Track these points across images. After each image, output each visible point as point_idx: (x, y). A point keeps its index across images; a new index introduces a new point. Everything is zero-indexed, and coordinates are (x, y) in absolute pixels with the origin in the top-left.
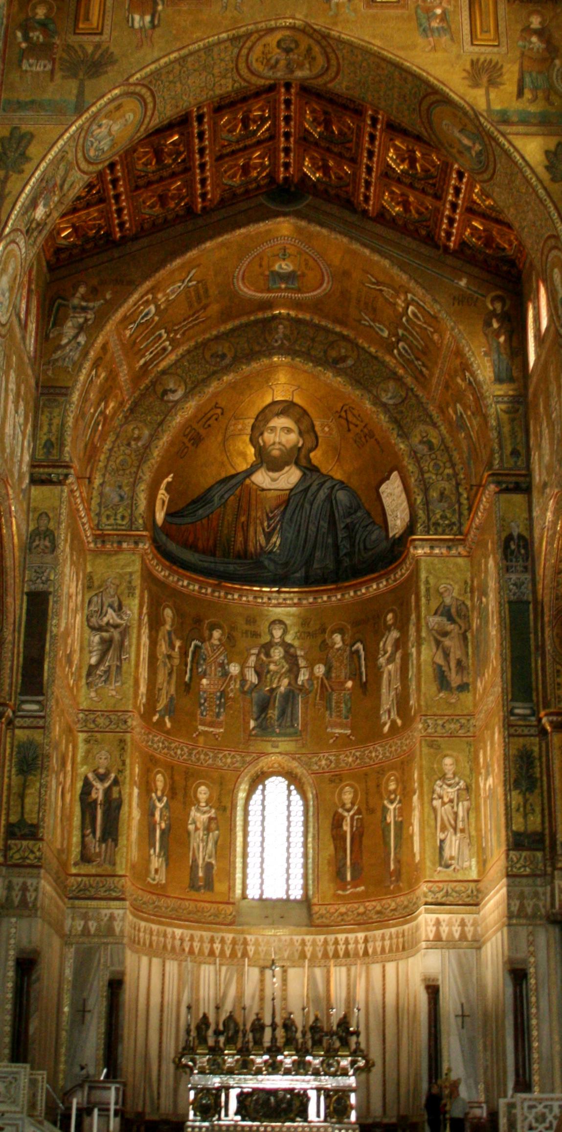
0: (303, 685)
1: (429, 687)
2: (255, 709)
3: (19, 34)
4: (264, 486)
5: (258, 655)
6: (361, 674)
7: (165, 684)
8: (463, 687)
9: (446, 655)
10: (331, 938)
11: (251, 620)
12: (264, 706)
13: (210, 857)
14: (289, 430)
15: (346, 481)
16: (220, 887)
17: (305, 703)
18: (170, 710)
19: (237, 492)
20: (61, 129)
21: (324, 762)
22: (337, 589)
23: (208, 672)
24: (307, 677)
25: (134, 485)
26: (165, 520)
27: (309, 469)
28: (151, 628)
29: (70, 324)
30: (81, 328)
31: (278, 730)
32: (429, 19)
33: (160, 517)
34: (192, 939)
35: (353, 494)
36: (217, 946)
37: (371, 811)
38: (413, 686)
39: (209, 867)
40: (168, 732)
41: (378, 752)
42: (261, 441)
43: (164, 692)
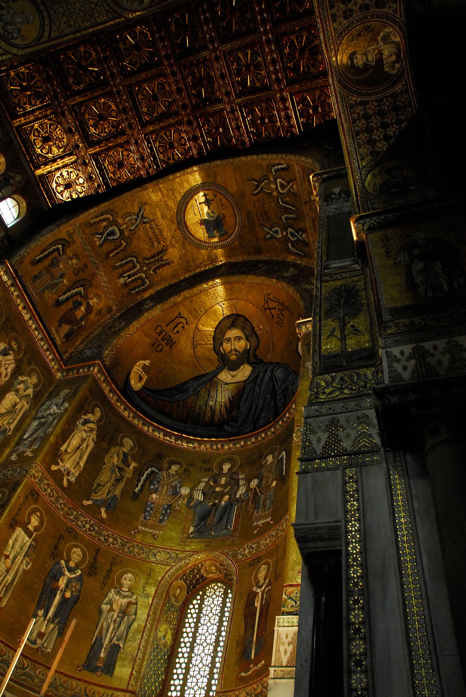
0: (240, 497)
2: (196, 518)
4: (227, 381)
5: (207, 483)
6: (282, 472)
7: (109, 485)
13: (118, 640)
14: (239, 338)
15: (279, 361)
19: (208, 386)
21: (247, 551)
23: (159, 489)
24: (243, 492)
31: (213, 533)
42: (221, 350)
43: (106, 489)
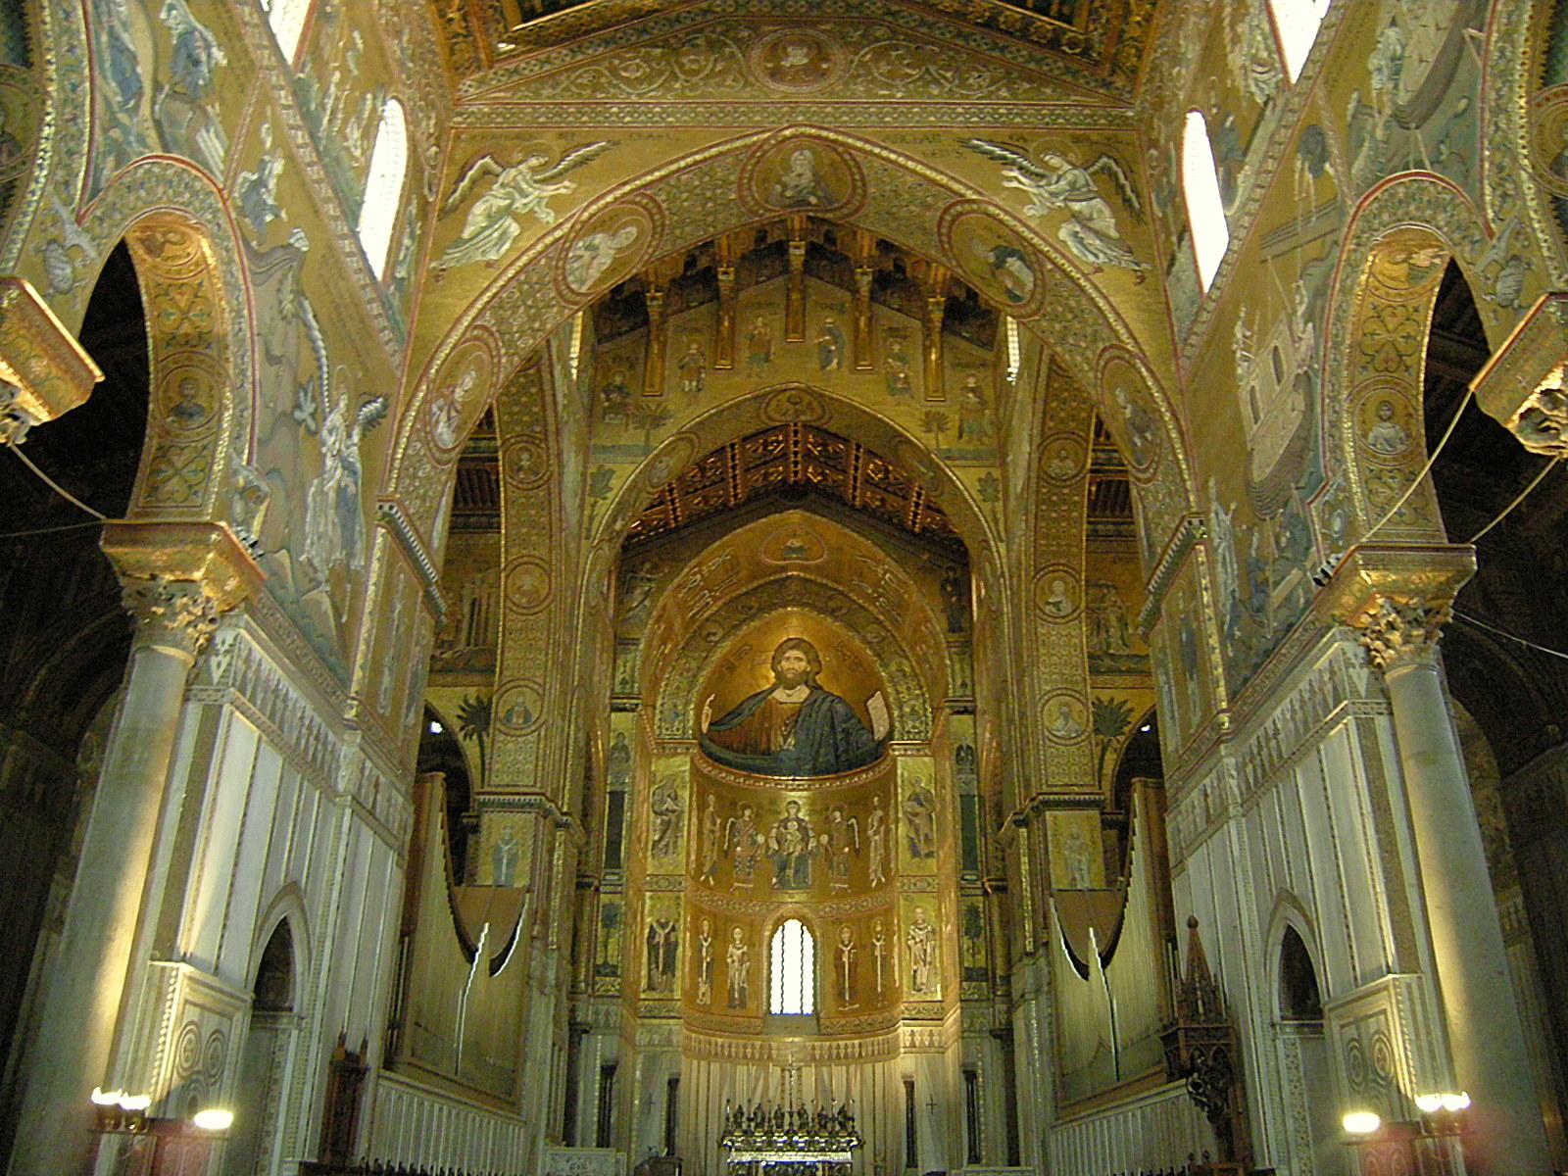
1: (904, 855)
3: (603, 396)
8: (929, 855)
9: (917, 831)
10: (835, 1044)
11: (773, 802)
12: (783, 867)
14: (800, 660)
16: (751, 1005)
17: (813, 864)
18: (713, 872)
20: (633, 467)
22: (837, 778)
25: (687, 704)
26: (709, 730)
27: (816, 688)
28: (699, 809)
29: (638, 591)
30: (647, 594)
32: (895, 382)
33: (705, 727)
34: (730, 1046)
35: (847, 705)
36: (749, 1050)
37: (864, 947)
38: (893, 854)
39: (742, 990)
40: (711, 889)
41: (867, 902)
